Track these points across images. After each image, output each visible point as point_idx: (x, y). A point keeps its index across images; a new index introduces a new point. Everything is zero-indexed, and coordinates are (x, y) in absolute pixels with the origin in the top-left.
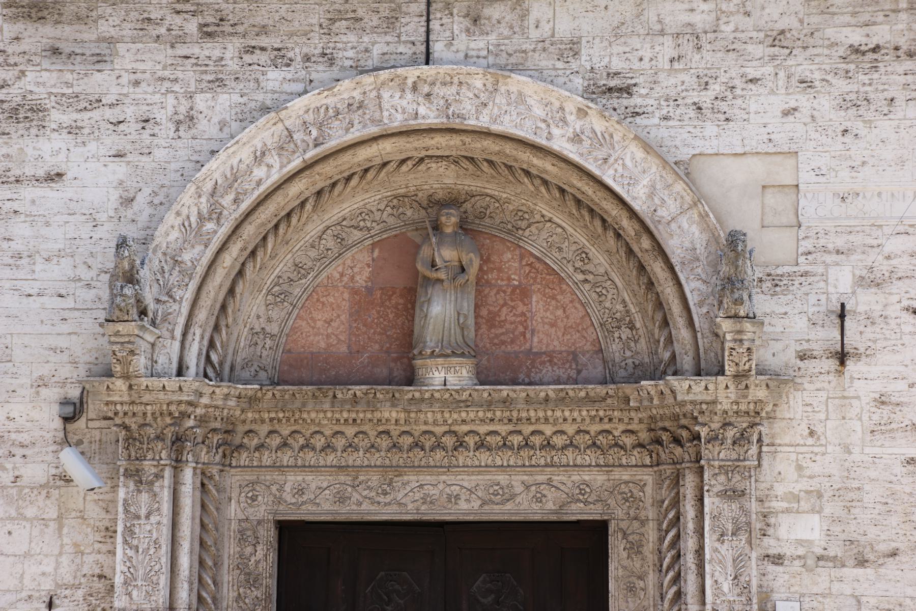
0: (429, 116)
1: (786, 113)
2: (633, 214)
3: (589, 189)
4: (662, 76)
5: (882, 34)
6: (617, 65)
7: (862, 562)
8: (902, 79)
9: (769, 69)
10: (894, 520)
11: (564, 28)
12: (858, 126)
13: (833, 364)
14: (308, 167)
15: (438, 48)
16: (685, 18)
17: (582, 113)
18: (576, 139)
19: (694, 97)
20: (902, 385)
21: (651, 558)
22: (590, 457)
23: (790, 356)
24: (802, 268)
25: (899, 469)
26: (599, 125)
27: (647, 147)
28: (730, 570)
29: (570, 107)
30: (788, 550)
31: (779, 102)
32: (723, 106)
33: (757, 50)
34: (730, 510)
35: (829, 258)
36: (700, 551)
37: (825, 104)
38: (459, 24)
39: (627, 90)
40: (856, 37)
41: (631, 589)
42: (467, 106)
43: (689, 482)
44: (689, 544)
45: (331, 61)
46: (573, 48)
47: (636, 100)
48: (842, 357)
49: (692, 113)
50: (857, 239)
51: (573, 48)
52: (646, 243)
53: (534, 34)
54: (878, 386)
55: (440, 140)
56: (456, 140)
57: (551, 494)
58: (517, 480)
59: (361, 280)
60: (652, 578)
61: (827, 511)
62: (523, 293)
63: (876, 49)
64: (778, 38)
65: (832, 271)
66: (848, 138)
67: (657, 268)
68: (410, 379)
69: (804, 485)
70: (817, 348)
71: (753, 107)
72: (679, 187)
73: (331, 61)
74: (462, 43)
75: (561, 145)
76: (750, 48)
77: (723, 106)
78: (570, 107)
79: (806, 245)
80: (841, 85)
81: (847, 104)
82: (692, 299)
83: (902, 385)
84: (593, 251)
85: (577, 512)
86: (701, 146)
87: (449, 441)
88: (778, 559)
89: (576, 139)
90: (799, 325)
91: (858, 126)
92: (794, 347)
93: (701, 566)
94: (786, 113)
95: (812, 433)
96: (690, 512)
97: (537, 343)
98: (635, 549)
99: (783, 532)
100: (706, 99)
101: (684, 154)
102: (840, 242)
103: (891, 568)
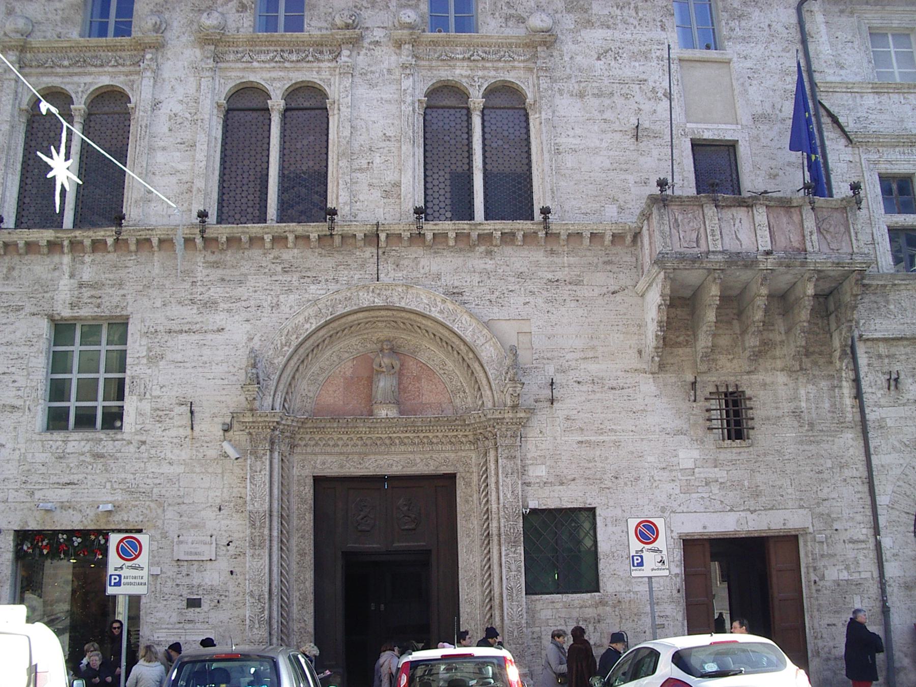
0: (379, 302)
1: (524, 304)
2: (465, 343)
3: (447, 333)
4: (475, 288)
5: (559, 275)
6: (456, 284)
7: (562, 484)
8: (568, 292)
9: (517, 287)
10: (573, 466)
11: (434, 268)
12: (553, 310)
13: (549, 404)
14: (327, 323)
15: (382, 276)
16: (483, 266)
17: (444, 301)
18: (441, 312)
19: (488, 297)
20: (575, 412)
21: (475, 488)
22: (449, 447)
23: (531, 401)
24: (535, 365)
25: (575, 446)
26: (451, 307)
27: (471, 315)
28: (510, 489)
29: (438, 299)
30: (532, 481)
31: (522, 300)
32: (500, 301)
33: (513, 280)
34: (510, 464)
35: (545, 362)
36: (497, 483)
37: (540, 301)
38: (390, 267)
39: (461, 294)
40: (550, 276)
41: (467, 501)
42: (396, 299)
43: (492, 454)
44: (492, 480)
45: (337, 282)
46: (438, 276)
47: (465, 298)
48: (552, 401)
49: (488, 303)
50: (555, 354)
51: (438, 276)
52: (471, 355)
53: (422, 271)
54: (566, 412)
55: (383, 313)
56: (390, 313)
57: (432, 462)
58: (418, 458)
59: (348, 374)
60: (475, 496)
61: (548, 464)
62: (418, 379)
63: (557, 281)
64: (520, 275)
65: (546, 366)
66: (550, 314)
67: (476, 366)
68: (371, 413)
69: (539, 453)
70: (542, 397)
71: (512, 302)
72: (485, 331)
73: (337, 282)
74: (392, 274)
75: (435, 314)
76: (509, 278)
77: (500, 301)
78: (438, 299)
79: (536, 356)
80: (545, 293)
81: (547, 301)
82: (491, 377)
83: (575, 412)
84: (447, 361)
85: (444, 470)
86: (492, 316)
87: (388, 442)
88: (528, 484)
89: (441, 312)
90: (535, 388)
91: (553, 310)
92: (533, 398)
93: (497, 489)
94: (524, 304)
95: (541, 432)
96: (492, 466)
97: (425, 399)
98: (468, 484)
99: (530, 473)
100: (493, 297)
101: (486, 319)
102: (549, 355)
103: (572, 486)
